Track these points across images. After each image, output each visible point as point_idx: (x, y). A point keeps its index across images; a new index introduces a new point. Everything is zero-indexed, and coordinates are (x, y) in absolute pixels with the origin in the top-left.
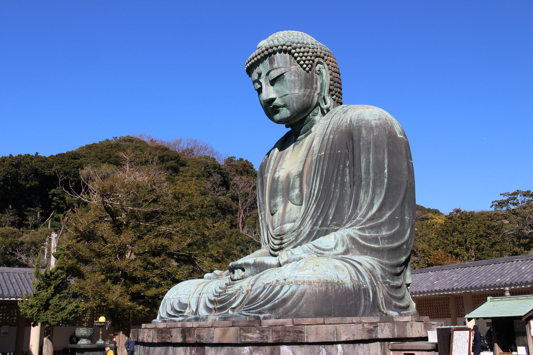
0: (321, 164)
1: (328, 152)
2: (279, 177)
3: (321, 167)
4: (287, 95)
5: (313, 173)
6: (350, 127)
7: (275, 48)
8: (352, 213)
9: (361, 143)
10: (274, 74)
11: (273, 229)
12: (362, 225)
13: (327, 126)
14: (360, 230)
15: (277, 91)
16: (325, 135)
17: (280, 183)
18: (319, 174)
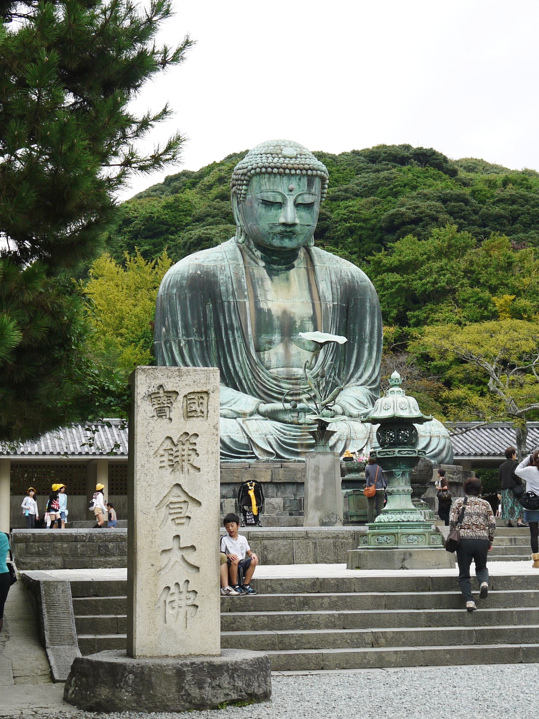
0: (336, 314)
1: (339, 303)
2: (269, 310)
3: (336, 318)
4: (310, 226)
5: (330, 322)
6: (353, 282)
7: (319, 172)
8: (353, 371)
9: (368, 304)
10: (308, 199)
11: (268, 368)
12: (369, 385)
13: (328, 272)
14: (370, 389)
15: (300, 217)
16: (331, 282)
17: (275, 318)
18: (335, 325)
